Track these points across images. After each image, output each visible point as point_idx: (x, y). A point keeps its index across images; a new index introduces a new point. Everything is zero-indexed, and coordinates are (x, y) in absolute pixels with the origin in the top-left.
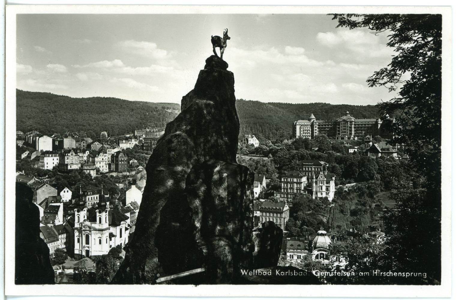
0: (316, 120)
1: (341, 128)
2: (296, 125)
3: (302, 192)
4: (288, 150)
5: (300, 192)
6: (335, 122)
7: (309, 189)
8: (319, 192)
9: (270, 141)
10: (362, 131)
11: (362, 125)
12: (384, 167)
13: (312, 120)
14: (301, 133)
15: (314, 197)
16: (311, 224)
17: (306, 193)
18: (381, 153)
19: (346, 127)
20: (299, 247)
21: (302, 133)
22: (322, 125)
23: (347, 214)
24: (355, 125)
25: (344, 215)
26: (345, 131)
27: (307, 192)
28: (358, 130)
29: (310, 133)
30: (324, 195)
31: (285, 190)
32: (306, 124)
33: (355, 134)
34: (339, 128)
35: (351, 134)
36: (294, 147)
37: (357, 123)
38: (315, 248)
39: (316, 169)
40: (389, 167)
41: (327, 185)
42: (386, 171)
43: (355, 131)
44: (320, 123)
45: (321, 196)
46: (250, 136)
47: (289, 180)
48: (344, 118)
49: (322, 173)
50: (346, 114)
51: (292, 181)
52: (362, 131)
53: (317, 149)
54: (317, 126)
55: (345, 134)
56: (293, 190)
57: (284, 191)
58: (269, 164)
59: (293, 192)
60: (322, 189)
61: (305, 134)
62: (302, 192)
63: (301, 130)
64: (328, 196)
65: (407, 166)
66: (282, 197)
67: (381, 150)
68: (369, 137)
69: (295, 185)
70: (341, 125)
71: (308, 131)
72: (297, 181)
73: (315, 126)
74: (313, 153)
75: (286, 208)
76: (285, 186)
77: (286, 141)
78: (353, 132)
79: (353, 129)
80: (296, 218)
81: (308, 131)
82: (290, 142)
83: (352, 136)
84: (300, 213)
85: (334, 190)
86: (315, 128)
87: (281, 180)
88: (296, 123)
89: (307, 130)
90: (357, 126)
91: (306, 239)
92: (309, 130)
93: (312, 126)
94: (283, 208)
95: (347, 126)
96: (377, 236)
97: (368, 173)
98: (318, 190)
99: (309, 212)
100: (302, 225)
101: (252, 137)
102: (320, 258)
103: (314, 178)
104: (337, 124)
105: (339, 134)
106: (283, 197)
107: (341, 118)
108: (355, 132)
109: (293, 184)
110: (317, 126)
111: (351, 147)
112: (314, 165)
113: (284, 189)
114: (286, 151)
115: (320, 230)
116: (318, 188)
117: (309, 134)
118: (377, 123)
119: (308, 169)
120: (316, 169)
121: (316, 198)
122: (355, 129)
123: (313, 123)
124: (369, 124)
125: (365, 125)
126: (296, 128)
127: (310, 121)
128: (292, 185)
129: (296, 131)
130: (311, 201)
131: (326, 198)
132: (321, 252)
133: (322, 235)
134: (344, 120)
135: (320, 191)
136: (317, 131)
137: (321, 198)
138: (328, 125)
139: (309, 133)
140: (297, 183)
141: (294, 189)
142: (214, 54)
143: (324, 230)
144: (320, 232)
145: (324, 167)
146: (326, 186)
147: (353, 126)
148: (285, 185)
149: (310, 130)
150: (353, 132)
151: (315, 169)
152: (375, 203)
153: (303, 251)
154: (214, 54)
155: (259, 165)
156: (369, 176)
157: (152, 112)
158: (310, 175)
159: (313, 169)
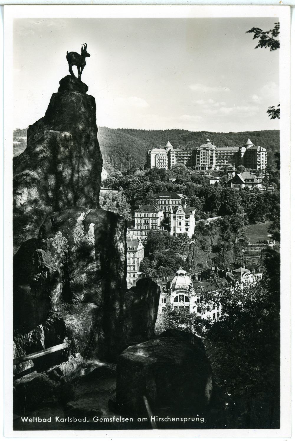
0: (173, 148)
1: (201, 157)
2: (150, 154)
3: (158, 228)
4: (142, 182)
5: (156, 228)
6: (194, 151)
8: (178, 227)
9: (120, 172)
10: (223, 160)
11: (224, 153)
12: (248, 199)
13: (169, 149)
14: (156, 162)
15: (172, 233)
16: (169, 263)
17: (162, 229)
18: (245, 184)
19: (206, 156)
21: (158, 162)
22: (180, 154)
23: (208, 250)
24: (216, 153)
25: (206, 252)
26: (205, 160)
27: (164, 228)
28: (219, 159)
29: (167, 162)
30: (183, 231)
31: (139, 227)
32: (161, 153)
33: (216, 163)
34: (199, 157)
35: (212, 163)
36: (148, 178)
37: (219, 152)
38: (174, 290)
39: (174, 202)
40: (253, 198)
42: (250, 203)
43: (216, 160)
44: (177, 152)
45: (179, 232)
47: (143, 216)
48: (205, 146)
49: (180, 207)
50: (206, 142)
51: (146, 216)
52: (223, 160)
53: (174, 180)
54: (175, 155)
55: (206, 163)
56: (148, 227)
57: (138, 227)
58: (120, 198)
60: (180, 224)
61: (160, 164)
63: (157, 159)
64: (187, 232)
65: (273, 198)
66: (135, 235)
67: (245, 180)
68: (232, 167)
70: (201, 154)
71: (165, 161)
72: (153, 216)
73: (171, 155)
74: (169, 184)
75: (141, 247)
76: (139, 222)
77: (138, 172)
78: (214, 162)
79: (214, 158)
80: (151, 258)
82: (143, 173)
83: (214, 166)
84: (156, 252)
86: (172, 158)
87: (133, 214)
88: (150, 152)
89: (163, 160)
90: (218, 155)
91: (163, 280)
92: (166, 160)
93: (169, 154)
94: (137, 247)
95: (208, 155)
96: (242, 273)
97: (230, 206)
98: (176, 226)
99: (166, 250)
100: (159, 264)
102: (180, 301)
103: (172, 212)
105: (199, 164)
108: (217, 162)
110: (174, 155)
111: (212, 178)
112: (172, 198)
113: (138, 225)
114: (139, 183)
115: (178, 269)
116: (177, 223)
117: (165, 164)
118: (239, 152)
120: (174, 202)
121: (174, 234)
122: (217, 158)
124: (231, 153)
125: (227, 153)
126: (150, 157)
128: (146, 221)
129: (150, 160)
130: (168, 237)
131: (186, 235)
132: (180, 294)
133: (181, 275)
134: (204, 149)
135: (179, 226)
137: (180, 234)
138: (187, 154)
139: (166, 163)
140: (153, 218)
142: (70, 74)
144: (179, 272)
145: (183, 200)
146: (186, 221)
147: (214, 155)
148: (139, 221)
149: (167, 159)
150: (214, 162)
154: (70, 74)
155: (108, 200)
156: (233, 208)
158: (167, 209)
159: (171, 203)
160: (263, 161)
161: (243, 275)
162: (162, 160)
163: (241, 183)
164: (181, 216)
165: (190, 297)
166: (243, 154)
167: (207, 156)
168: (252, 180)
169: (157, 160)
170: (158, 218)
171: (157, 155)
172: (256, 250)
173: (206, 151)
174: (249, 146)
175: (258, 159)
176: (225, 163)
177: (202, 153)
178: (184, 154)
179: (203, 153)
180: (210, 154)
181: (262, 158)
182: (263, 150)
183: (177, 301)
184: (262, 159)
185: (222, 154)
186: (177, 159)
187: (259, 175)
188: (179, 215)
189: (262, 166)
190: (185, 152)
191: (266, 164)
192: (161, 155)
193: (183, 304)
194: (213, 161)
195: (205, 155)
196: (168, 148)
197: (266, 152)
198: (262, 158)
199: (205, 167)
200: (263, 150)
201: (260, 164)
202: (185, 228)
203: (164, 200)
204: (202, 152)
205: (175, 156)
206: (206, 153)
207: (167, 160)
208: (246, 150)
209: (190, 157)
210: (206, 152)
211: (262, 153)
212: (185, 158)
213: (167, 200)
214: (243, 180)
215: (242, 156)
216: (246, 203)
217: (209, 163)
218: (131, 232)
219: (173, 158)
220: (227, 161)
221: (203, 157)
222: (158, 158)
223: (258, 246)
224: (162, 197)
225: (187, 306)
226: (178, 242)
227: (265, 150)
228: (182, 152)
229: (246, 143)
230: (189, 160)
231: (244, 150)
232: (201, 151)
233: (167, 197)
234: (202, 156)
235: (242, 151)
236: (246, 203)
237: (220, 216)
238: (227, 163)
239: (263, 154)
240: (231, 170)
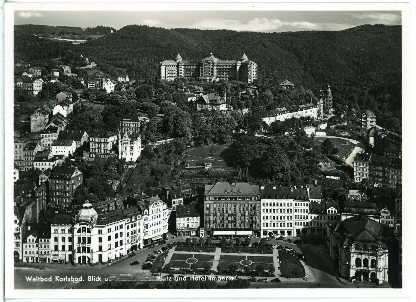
0: (183, 60)
1: (204, 70)
3: (109, 152)
5: (107, 152)
6: (199, 63)
7: (115, 148)
11: (223, 66)
12: (198, 123)
13: (178, 61)
14: (166, 73)
18: (210, 104)
20: (65, 221)
23: (146, 174)
24: (217, 66)
25: (143, 175)
26: (208, 72)
29: (176, 73)
31: (94, 150)
32: (171, 64)
33: (217, 75)
34: (202, 69)
35: (213, 75)
36: (136, 95)
38: (78, 222)
39: (134, 125)
41: (132, 145)
42: (199, 126)
43: (217, 72)
46: (104, 80)
47: (97, 141)
48: (208, 59)
49: (126, 134)
50: (209, 56)
51: (99, 141)
56: (100, 150)
57: (93, 151)
59: (100, 152)
60: (126, 149)
61: (170, 74)
62: (109, 152)
63: (166, 70)
65: (220, 122)
67: (210, 101)
69: (102, 145)
70: (204, 67)
71: (174, 72)
72: (104, 141)
73: (180, 66)
76: (94, 146)
78: (215, 74)
79: (215, 71)
81: (170, 72)
83: (214, 78)
85: (141, 149)
86: (180, 69)
88: (161, 63)
89: (173, 71)
90: (219, 67)
92: (175, 71)
93: (178, 66)
96: (151, 203)
97: (180, 129)
98: (123, 151)
101: (107, 81)
102: (82, 232)
104: (200, 65)
105: (202, 75)
106: (92, 157)
107: (205, 59)
108: (218, 73)
109: (100, 144)
111: (191, 95)
112: (132, 121)
113: (92, 149)
114: (126, 100)
116: (123, 148)
117: (174, 75)
118: (235, 66)
119: (127, 125)
121: (121, 158)
122: (218, 70)
123: (178, 63)
124: (229, 66)
126: (161, 69)
127: (175, 61)
129: (161, 71)
132: (84, 226)
133: (86, 208)
134: (207, 62)
135: (125, 151)
136: (182, 72)
138: (193, 66)
139: (175, 74)
141: (101, 149)
143: (90, 202)
144: (85, 205)
147: (215, 68)
148: (94, 145)
149: (176, 70)
150: (215, 74)
151: (133, 125)
152: (181, 160)
153: (67, 225)
156: (183, 132)
157: (34, 42)
159: (132, 125)
161: (151, 205)
162: (172, 72)
163: (205, 103)
164: (127, 141)
165: (91, 229)
166: (238, 68)
168: (215, 101)
170: (108, 143)
171: (167, 66)
172: (192, 172)
173: (208, 64)
176: (225, 75)
178: (190, 66)
180: (211, 66)
181: (252, 71)
183: (80, 233)
184: (252, 73)
186: (185, 70)
187: (223, 96)
188: (125, 141)
189: (252, 79)
190: (192, 64)
192: (171, 66)
193: (84, 235)
198: (252, 71)
202: (130, 153)
203: (126, 122)
208: (241, 64)
209: (195, 69)
211: (252, 67)
212: (192, 69)
213: (129, 122)
214: (207, 101)
215: (238, 69)
216: (196, 126)
218: (88, 155)
219: (181, 69)
220: (226, 74)
221: (205, 69)
223: (196, 168)
224: (124, 119)
225: (88, 236)
226: (111, 170)
227: (255, 64)
230: (195, 71)
231: (239, 63)
232: (204, 64)
233: (128, 120)
235: (238, 65)
236: (196, 126)
237: (172, 138)
238: (226, 75)
239: (253, 68)
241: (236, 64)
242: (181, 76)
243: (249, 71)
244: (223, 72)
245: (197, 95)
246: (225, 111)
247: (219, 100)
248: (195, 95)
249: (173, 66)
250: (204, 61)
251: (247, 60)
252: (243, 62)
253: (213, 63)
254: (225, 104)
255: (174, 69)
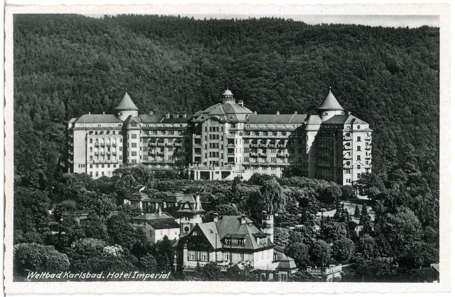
0: (139, 113)
1: (204, 143)
2: (72, 131)
19: (218, 138)
22: (155, 130)
26: (216, 150)
28: (255, 149)
29: (120, 153)
32: (103, 125)
33: (246, 159)
34: (198, 141)
35: (231, 160)
37: (253, 126)
43: (246, 150)
48: (217, 109)
50: (220, 99)
61: (101, 159)
63: (89, 145)
67: (223, 241)
70: (204, 134)
71: (113, 150)
73: (130, 133)
78: (239, 155)
79: (240, 146)
81: (102, 150)
86: (131, 141)
88: (73, 124)
89: (109, 147)
90: (252, 135)
92: (115, 146)
93: (124, 132)
105: (198, 159)
107: (206, 111)
122: (247, 146)
123: (126, 123)
124: (284, 132)
126: (72, 140)
129: (72, 149)
138: (172, 130)
160: (359, 158)
162: (106, 148)
163: (209, 248)
167: (220, 138)
169: (91, 148)
171: (91, 133)
173: (217, 124)
174: (328, 112)
175: (344, 152)
176: (269, 159)
177: (206, 131)
178: (163, 130)
179: (208, 129)
180: (227, 132)
181: (355, 148)
182: (359, 127)
184: (355, 153)
185: (261, 135)
189: (356, 172)
190: (168, 125)
191: (368, 166)
194: (234, 154)
195: (214, 135)
196: (124, 113)
197: (370, 133)
199: (211, 171)
200: (359, 127)
201: (349, 167)
204: (206, 128)
205: (142, 135)
206: (218, 131)
207: (118, 148)
208: (323, 124)
209: (179, 140)
210: (218, 128)
211: (355, 136)
212: (166, 141)
214: (213, 240)
217: (226, 160)
222: (94, 141)
227: (365, 126)
228: (159, 125)
229: (322, 104)
232: (204, 125)
234: (206, 139)
235: (310, 127)
239: (359, 139)
240: (189, 211)
241: (304, 126)
242: (134, 161)
243: (346, 147)
244: (265, 152)
245: (183, 220)
246: (270, 272)
247: (253, 238)
248: (178, 221)
249: (108, 133)
250: (206, 117)
251: (339, 113)
252: (326, 118)
253: (233, 123)
254: (272, 251)
255: (113, 141)
